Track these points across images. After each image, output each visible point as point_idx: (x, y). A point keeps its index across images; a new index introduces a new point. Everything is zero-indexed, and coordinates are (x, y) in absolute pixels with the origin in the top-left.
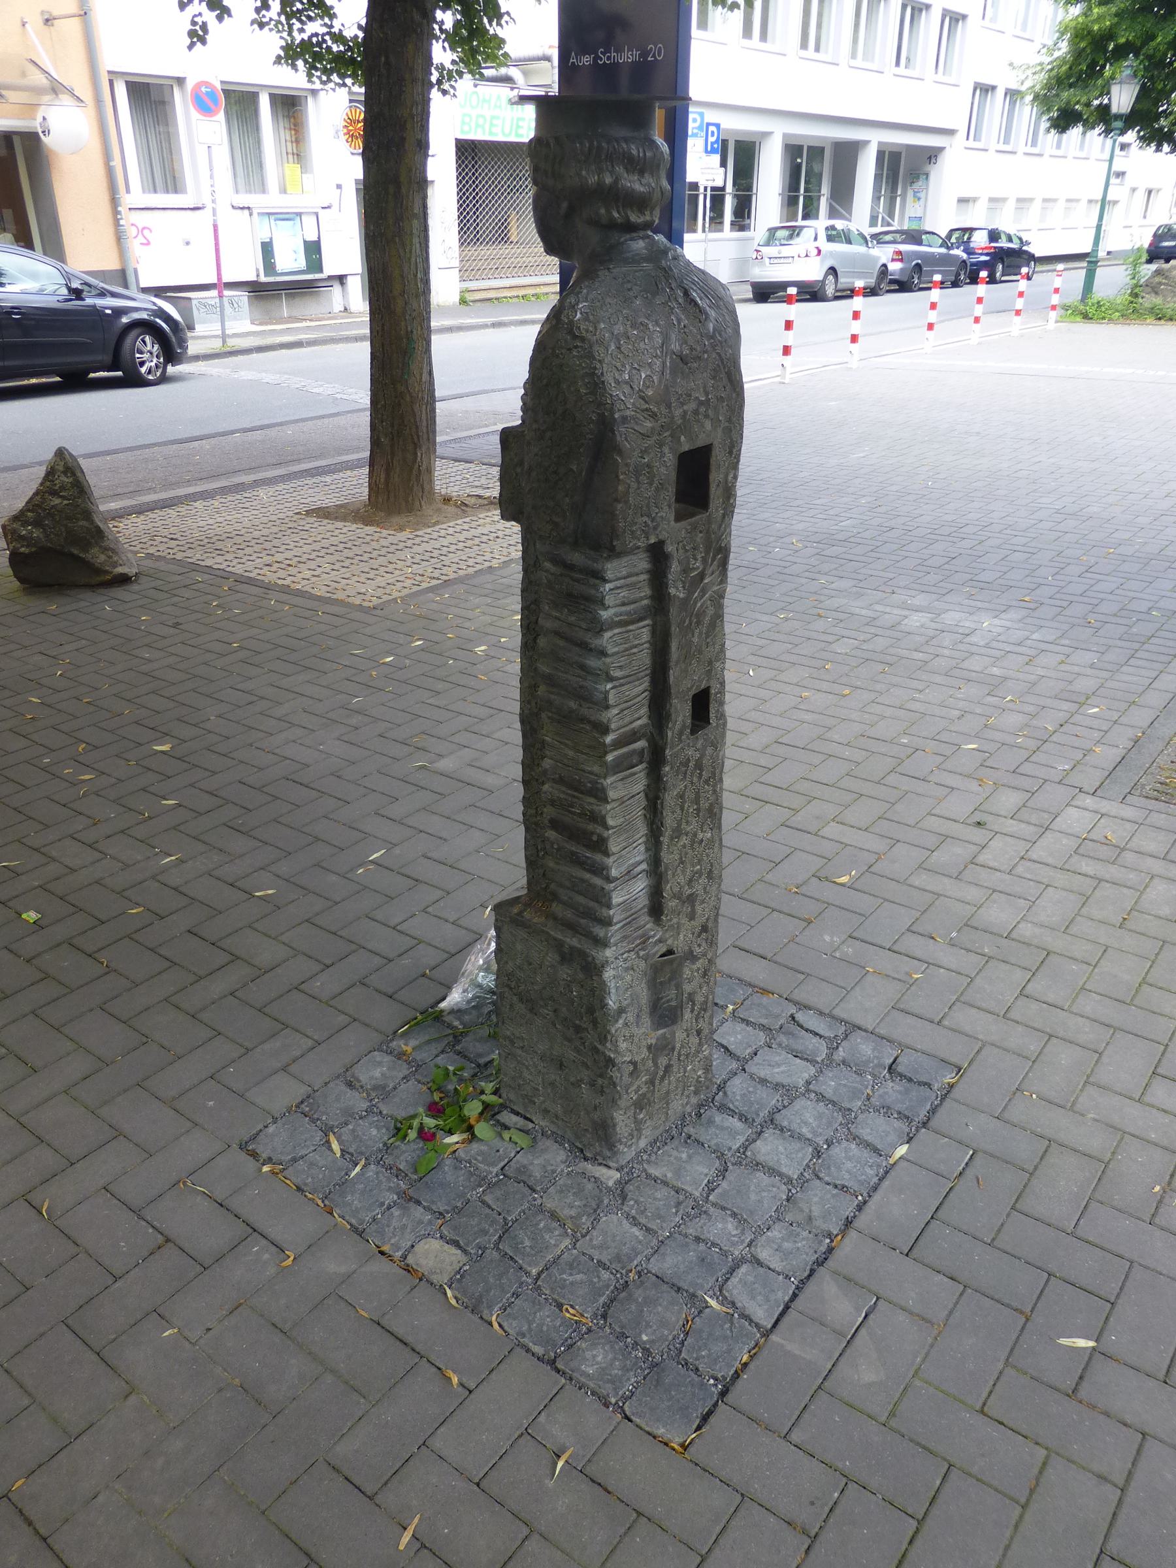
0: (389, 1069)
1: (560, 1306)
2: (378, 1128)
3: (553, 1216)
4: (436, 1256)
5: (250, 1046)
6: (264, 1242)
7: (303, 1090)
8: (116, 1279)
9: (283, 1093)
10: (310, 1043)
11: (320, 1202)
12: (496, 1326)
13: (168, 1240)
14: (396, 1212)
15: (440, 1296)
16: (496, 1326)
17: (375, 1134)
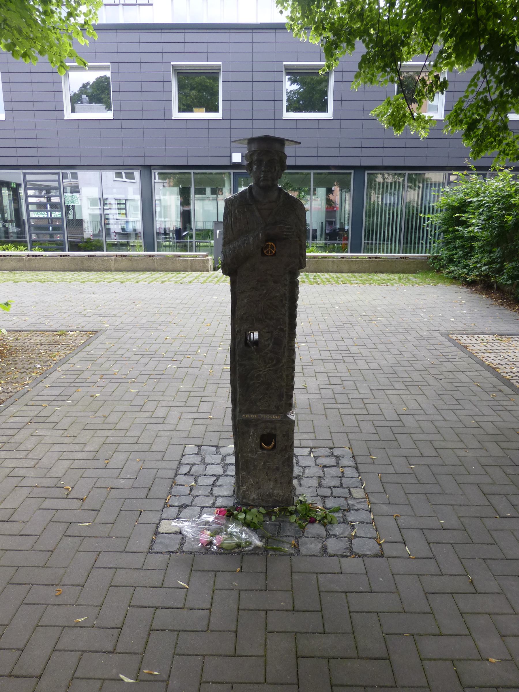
0: (307, 544)
1: (343, 472)
2: (334, 529)
3: (320, 484)
4: (358, 493)
5: (344, 594)
6: (400, 524)
7: (342, 560)
8: (452, 544)
9: (351, 564)
10: (320, 576)
11: (374, 524)
12: (360, 477)
13: (429, 544)
14: (356, 508)
15: (366, 488)
16: (360, 477)
17: (337, 529)
